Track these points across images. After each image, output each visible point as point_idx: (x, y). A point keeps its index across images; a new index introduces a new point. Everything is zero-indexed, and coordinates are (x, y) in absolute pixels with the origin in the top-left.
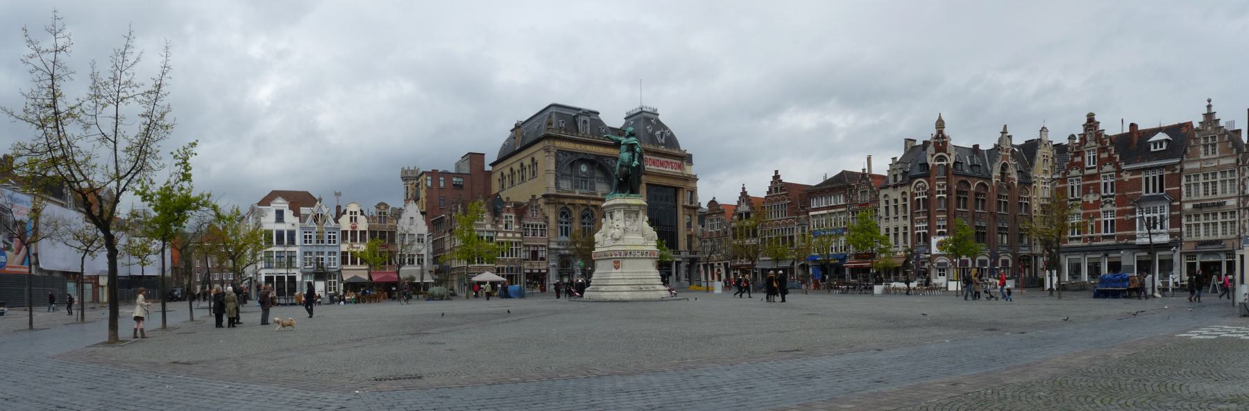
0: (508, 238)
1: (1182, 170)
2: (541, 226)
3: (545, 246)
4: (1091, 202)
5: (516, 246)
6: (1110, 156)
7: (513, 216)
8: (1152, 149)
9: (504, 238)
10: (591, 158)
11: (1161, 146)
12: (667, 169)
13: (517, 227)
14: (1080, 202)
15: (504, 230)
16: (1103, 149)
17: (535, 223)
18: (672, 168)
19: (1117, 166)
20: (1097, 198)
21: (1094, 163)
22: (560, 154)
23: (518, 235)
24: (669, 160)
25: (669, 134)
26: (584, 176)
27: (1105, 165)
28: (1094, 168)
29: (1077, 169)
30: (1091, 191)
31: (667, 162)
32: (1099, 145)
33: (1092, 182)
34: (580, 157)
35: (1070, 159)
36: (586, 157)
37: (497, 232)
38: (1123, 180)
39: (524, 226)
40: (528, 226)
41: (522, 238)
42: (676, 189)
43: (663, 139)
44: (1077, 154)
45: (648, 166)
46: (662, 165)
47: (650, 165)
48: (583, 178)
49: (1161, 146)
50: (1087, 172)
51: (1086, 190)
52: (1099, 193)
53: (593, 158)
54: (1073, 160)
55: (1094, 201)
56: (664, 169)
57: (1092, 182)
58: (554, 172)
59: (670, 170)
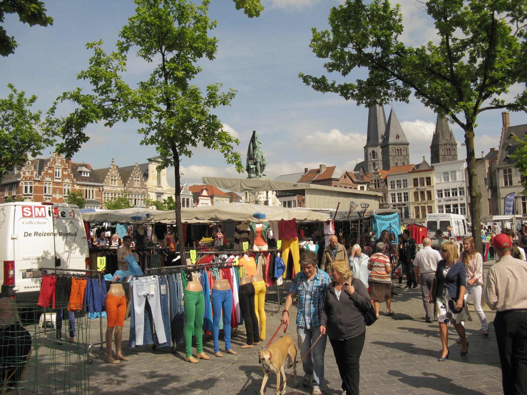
1: (103, 190)
4: (58, 198)
6: (69, 174)
8: (83, 175)
11: (87, 175)
14: (51, 198)
16: (65, 169)
19: (72, 179)
20: (61, 197)
21: (59, 176)
27: (66, 178)
28: (60, 179)
29: (50, 177)
30: (58, 192)
32: (63, 166)
33: (58, 187)
35: (46, 170)
38: (75, 189)
44: (50, 168)
49: (87, 175)
50: (56, 180)
51: (54, 191)
52: (62, 194)
54: (47, 171)
55: (59, 198)
57: (58, 187)
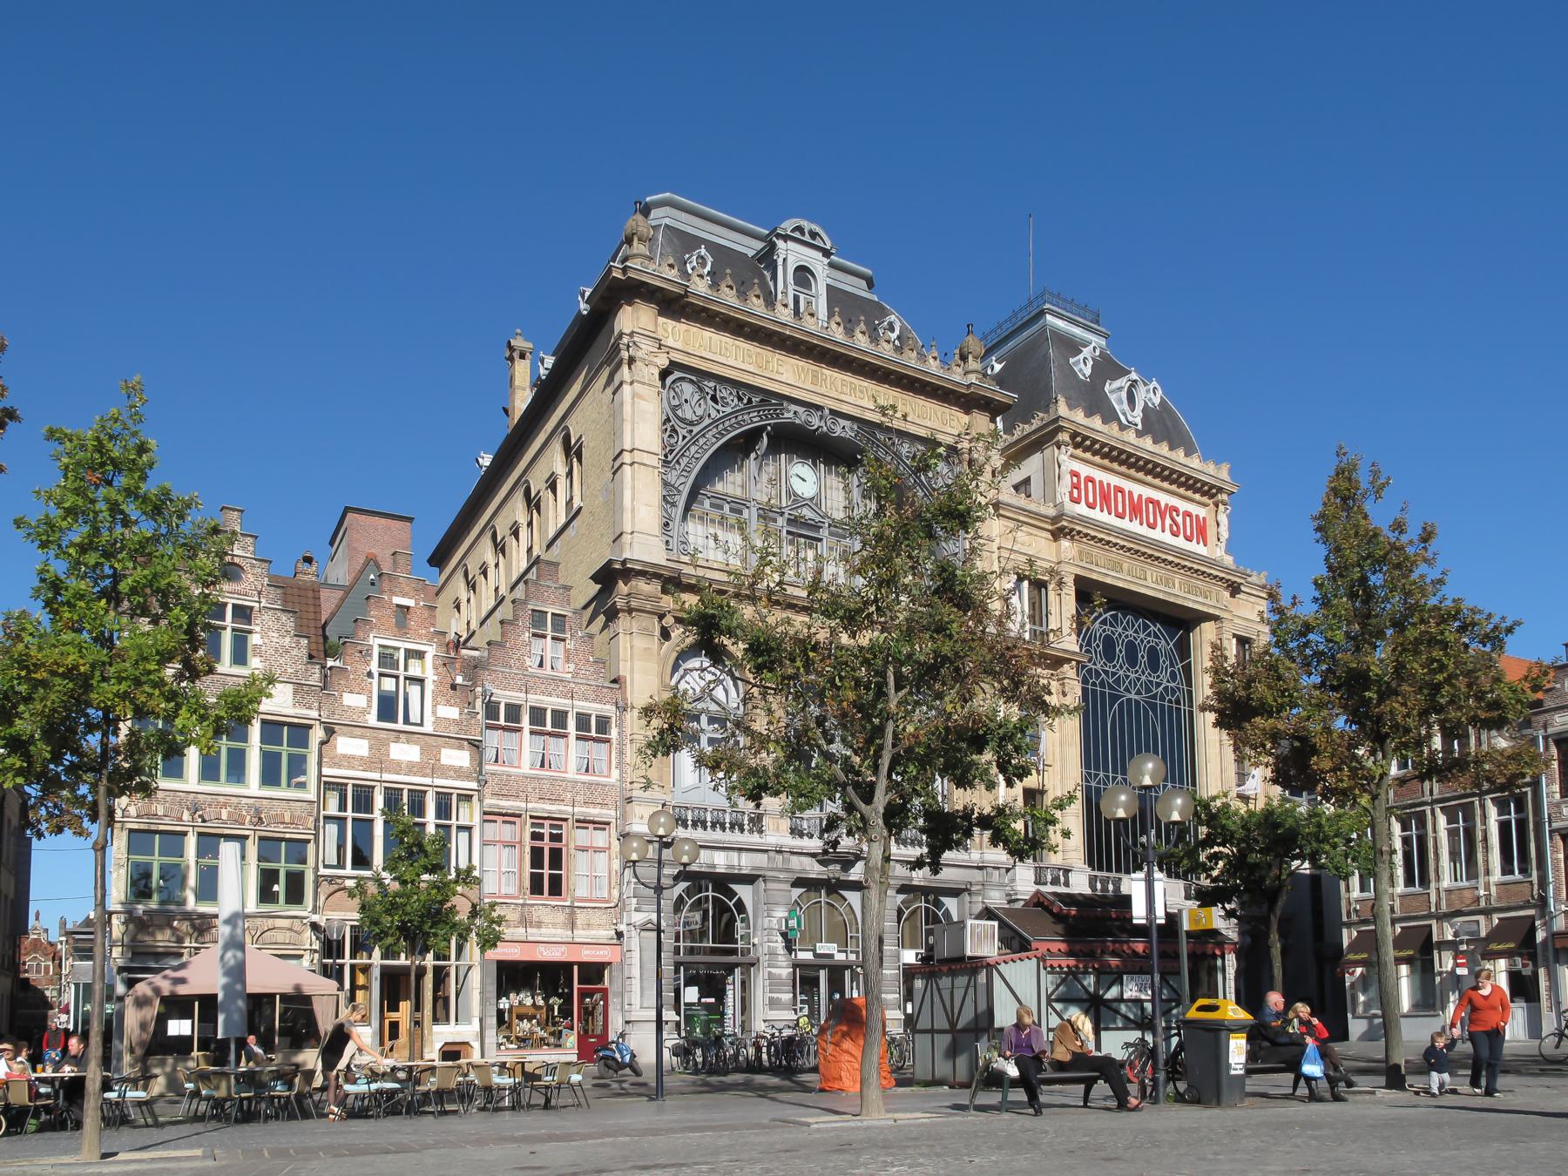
0: (397, 767)
2: (583, 721)
3: (601, 825)
5: (444, 810)
7: (431, 651)
9: (367, 764)
10: (838, 432)
12: (1156, 534)
13: (452, 713)
15: (372, 719)
17: (551, 702)
18: (1175, 534)
22: (687, 389)
23: (459, 758)
24: (1165, 499)
25: (1157, 401)
26: (807, 513)
31: (1156, 503)
34: (791, 414)
36: (815, 422)
37: (330, 731)
39: (491, 710)
40: (514, 712)
41: (478, 772)
42: (1180, 622)
43: (1138, 411)
45: (1082, 509)
46: (1136, 510)
47: (1091, 506)
48: (806, 525)
53: (850, 434)
56: (1143, 530)
58: (654, 461)
59: (1167, 537)
